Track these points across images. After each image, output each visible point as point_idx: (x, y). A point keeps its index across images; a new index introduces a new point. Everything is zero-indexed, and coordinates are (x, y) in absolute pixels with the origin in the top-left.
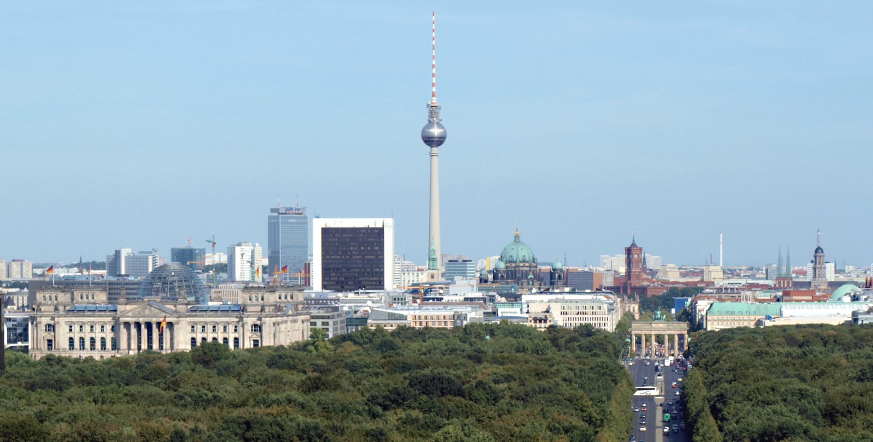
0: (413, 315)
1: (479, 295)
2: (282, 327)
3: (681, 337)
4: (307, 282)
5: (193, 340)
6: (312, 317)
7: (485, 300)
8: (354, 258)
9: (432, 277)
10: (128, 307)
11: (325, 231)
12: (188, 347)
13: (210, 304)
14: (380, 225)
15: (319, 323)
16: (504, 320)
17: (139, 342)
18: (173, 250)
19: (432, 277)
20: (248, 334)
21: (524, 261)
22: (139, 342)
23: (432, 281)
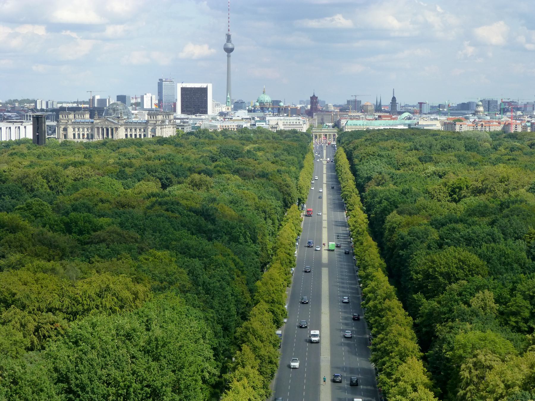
0: (220, 125)
1: (248, 117)
2: (164, 129)
3: (334, 135)
4: (175, 111)
5: (126, 135)
6: (177, 126)
7: (250, 119)
8: (195, 101)
9: (228, 109)
10: (98, 121)
11: (183, 89)
12: (124, 137)
13: (133, 119)
14: (205, 87)
15: (180, 128)
16: (259, 127)
17: (103, 134)
18: (118, 96)
19: (228, 109)
20: (149, 133)
21: (267, 103)
22: (103, 134)
23: (227, 111)
